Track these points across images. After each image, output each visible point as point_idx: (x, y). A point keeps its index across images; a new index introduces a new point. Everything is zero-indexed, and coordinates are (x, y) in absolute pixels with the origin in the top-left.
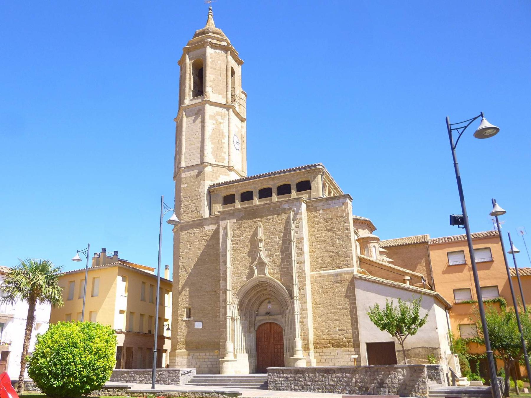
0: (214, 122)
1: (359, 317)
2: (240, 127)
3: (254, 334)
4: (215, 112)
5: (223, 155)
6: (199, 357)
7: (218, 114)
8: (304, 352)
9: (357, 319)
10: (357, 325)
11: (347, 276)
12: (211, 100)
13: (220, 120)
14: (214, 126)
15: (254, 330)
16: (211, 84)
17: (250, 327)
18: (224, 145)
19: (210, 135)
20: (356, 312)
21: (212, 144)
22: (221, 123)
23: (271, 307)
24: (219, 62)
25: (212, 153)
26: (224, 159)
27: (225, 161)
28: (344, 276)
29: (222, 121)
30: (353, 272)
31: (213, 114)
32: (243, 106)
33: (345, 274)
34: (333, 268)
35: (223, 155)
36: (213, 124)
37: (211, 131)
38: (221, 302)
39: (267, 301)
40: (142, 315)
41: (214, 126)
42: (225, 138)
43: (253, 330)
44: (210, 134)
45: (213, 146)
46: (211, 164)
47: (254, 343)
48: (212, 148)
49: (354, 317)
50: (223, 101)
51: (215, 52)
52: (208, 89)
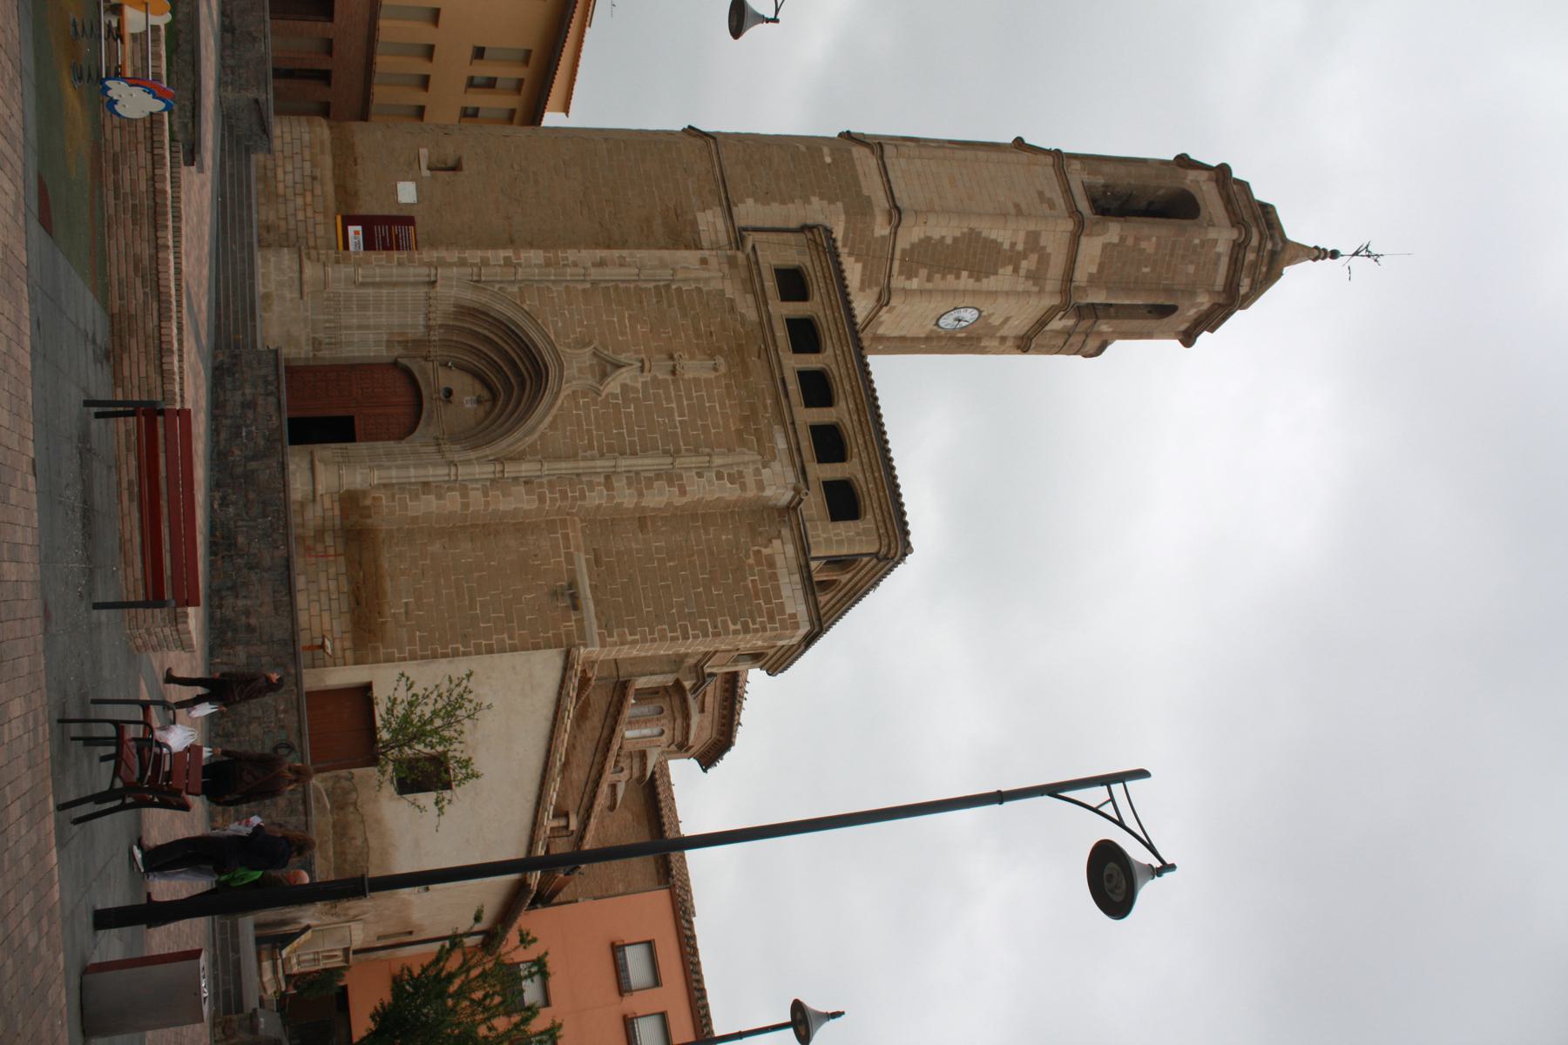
0: (1020, 247)
1: (450, 662)
2: (1004, 332)
3: (385, 354)
4: (1049, 250)
5: (924, 272)
6: (309, 195)
7: (1044, 259)
8: (336, 497)
9: (445, 656)
10: (423, 657)
11: (574, 628)
12: (1084, 240)
13: (1024, 264)
14: (1006, 246)
15: (396, 354)
16: (1130, 242)
17: (404, 343)
18: (953, 276)
19: (980, 233)
20: (465, 654)
21: (955, 239)
22: (1016, 270)
23: (469, 406)
25: (928, 239)
26: (910, 275)
27: (903, 277)
28: (573, 618)
29: (1022, 272)
30: (586, 646)
31: (1042, 243)
32: (1065, 344)
33: (580, 621)
34: (594, 588)
35: (924, 272)
36: (1013, 245)
37: (993, 236)
38: (479, 253)
39: (486, 394)
40: (429, 52)
41: (1006, 246)
42: (972, 280)
43: (398, 351)
44: (983, 235)
45: (949, 241)
46: (895, 233)
47: (356, 354)
48: (943, 238)
49: (447, 648)
50: (1080, 276)
51: (1219, 255)
52: (1114, 231)
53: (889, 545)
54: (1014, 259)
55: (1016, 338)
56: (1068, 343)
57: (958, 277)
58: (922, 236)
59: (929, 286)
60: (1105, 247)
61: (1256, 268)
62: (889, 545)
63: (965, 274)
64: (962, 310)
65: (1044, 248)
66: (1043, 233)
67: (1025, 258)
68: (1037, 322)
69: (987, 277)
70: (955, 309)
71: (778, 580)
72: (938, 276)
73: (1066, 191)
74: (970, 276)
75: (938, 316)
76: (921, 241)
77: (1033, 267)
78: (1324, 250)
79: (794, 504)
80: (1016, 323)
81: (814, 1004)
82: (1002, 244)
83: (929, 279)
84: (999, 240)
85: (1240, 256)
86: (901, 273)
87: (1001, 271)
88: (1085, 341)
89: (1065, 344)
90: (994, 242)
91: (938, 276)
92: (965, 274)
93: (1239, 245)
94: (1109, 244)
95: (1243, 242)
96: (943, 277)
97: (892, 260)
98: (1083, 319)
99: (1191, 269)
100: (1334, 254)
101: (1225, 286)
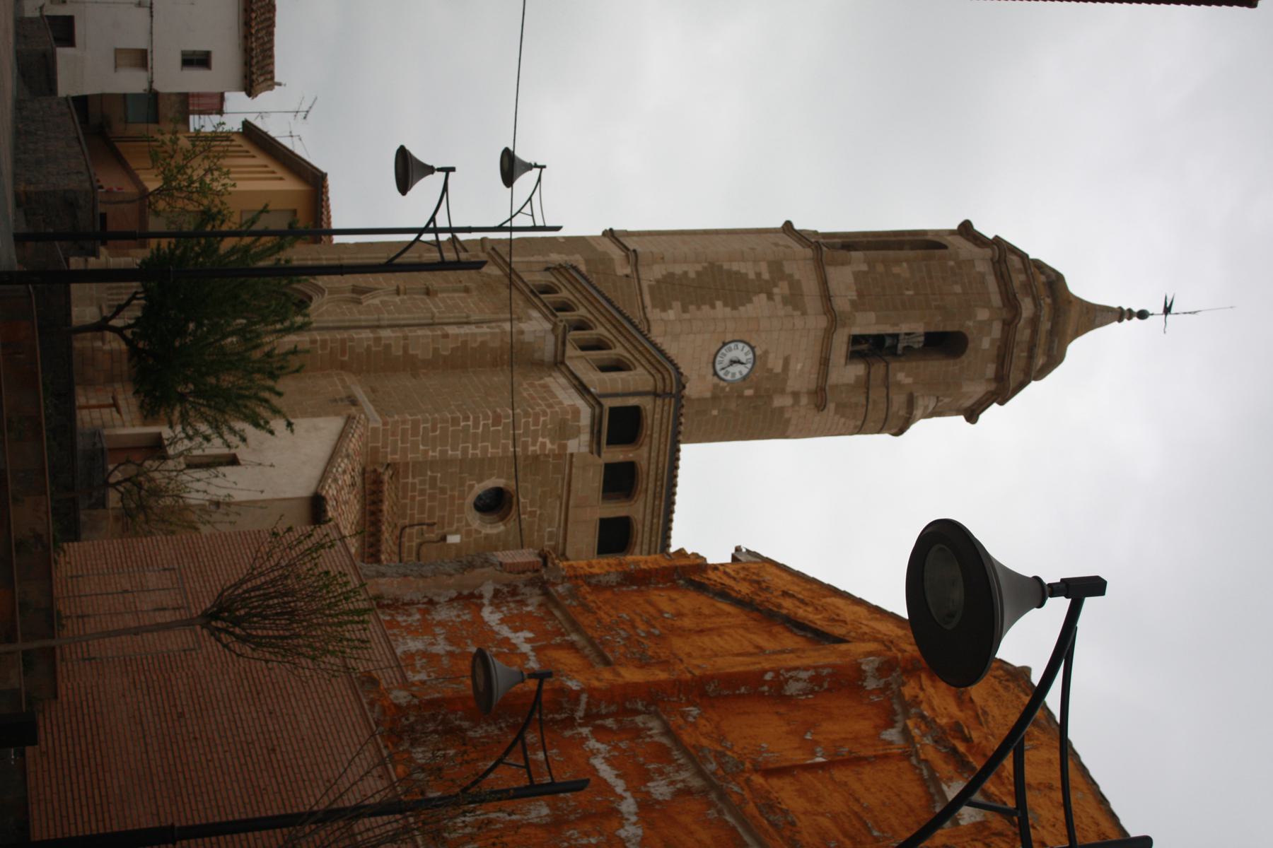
0: (766, 276)
4: (797, 277)
5: (677, 305)
7: (795, 286)
13: (776, 290)
14: (752, 276)
22: (770, 297)
24: (958, 289)
25: (672, 275)
26: (664, 308)
27: (658, 310)
29: (778, 298)
35: (677, 305)
36: (758, 275)
41: (752, 276)
45: (692, 275)
46: (637, 270)
48: (686, 273)
53: (664, 379)
54: (766, 289)
55: (810, 393)
56: (870, 400)
57: (713, 307)
58: (664, 273)
59: (687, 316)
60: (857, 276)
61: (1031, 287)
62: (664, 379)
63: (719, 304)
64: (732, 345)
65: (791, 276)
66: (785, 263)
67: (776, 286)
68: (820, 364)
69: (743, 305)
70: (724, 344)
71: (557, 398)
72: (692, 308)
73: (800, 239)
74: (725, 305)
75: (711, 360)
76: (665, 277)
77: (786, 291)
78: (1130, 310)
79: (559, 358)
80: (799, 366)
81: (522, 154)
82: (746, 274)
83: (685, 310)
84: (743, 271)
85: (1004, 269)
86: (654, 306)
87: (755, 299)
88: (888, 395)
89: (867, 401)
90: (737, 273)
91: (692, 308)
92: (719, 304)
93: (998, 261)
94: (859, 272)
95: (1000, 257)
96: (699, 308)
97: (641, 294)
98: (873, 365)
99: (958, 289)
100: (1143, 315)
101: (1003, 300)
